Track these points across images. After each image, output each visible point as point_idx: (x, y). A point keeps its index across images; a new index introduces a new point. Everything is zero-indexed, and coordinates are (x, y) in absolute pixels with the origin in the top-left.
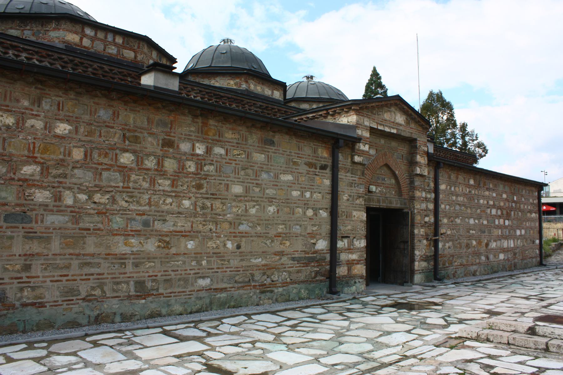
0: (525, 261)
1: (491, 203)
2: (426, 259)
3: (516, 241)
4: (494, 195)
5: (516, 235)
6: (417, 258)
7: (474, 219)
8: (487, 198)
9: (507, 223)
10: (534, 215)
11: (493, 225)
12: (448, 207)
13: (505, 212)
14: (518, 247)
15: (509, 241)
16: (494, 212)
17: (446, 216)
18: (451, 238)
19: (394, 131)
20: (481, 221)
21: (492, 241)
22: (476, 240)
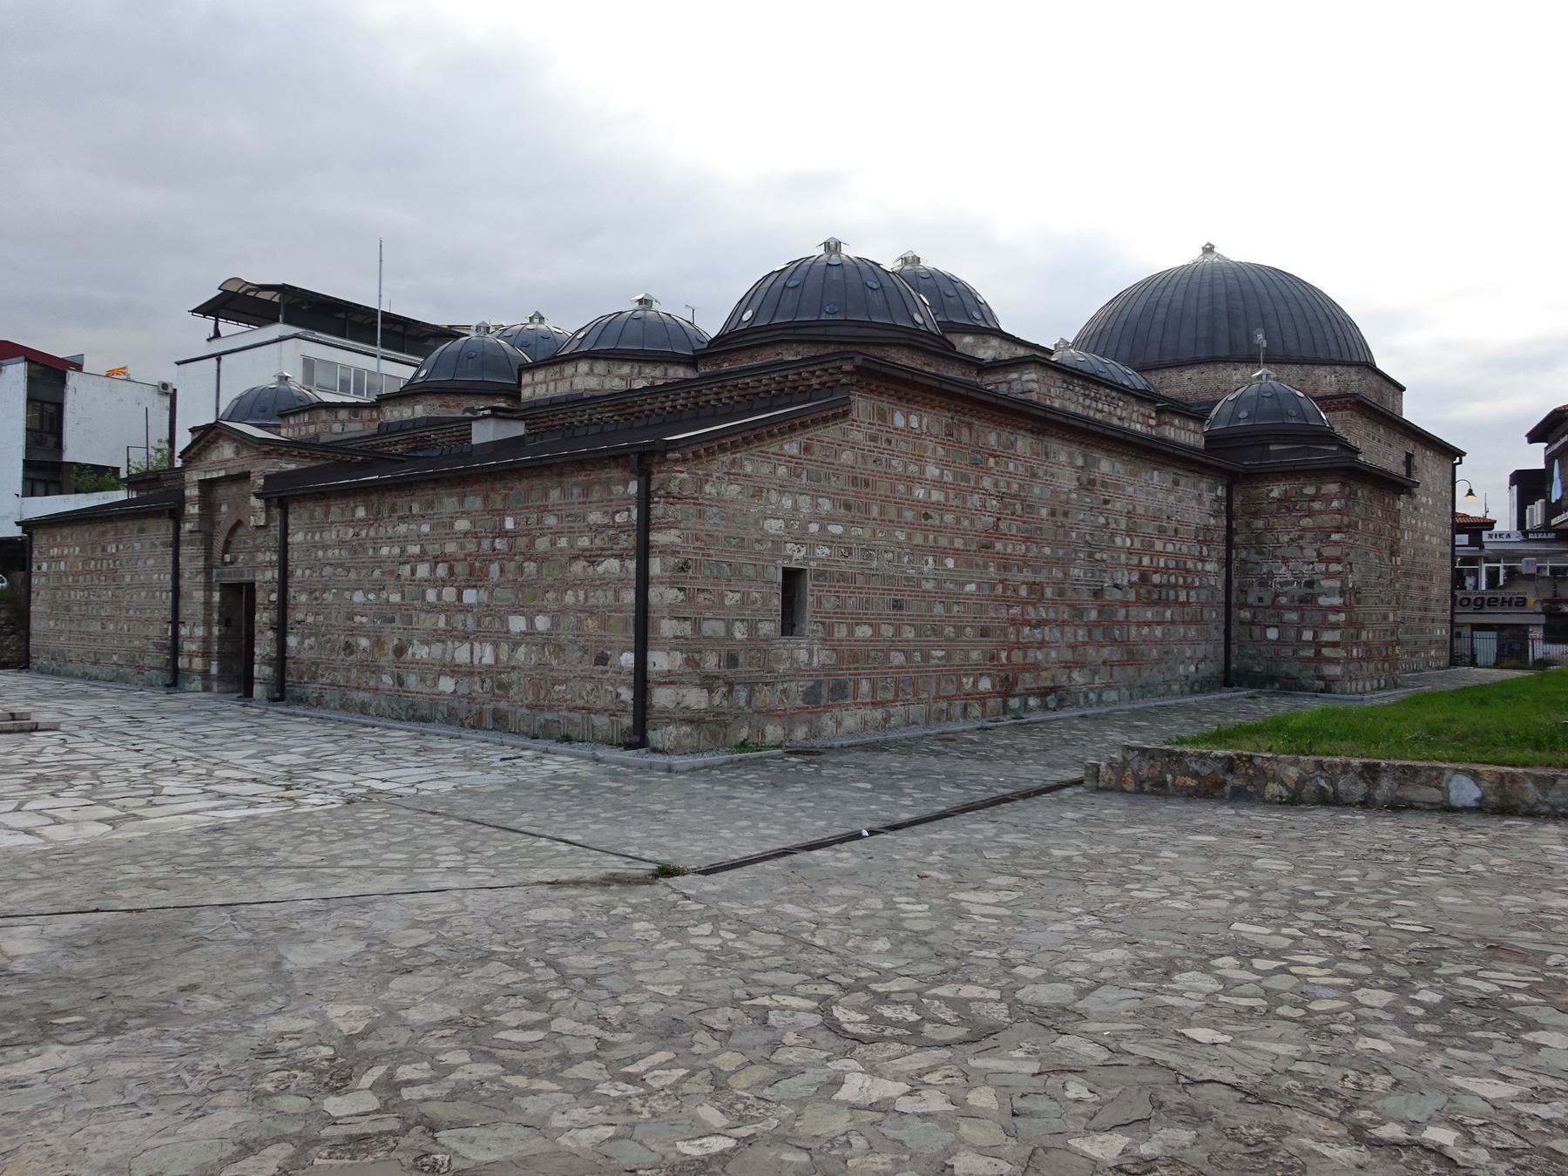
0: (549, 716)
1: (415, 549)
2: (268, 662)
3: (505, 648)
4: (425, 528)
5: (508, 632)
6: (257, 659)
7: (366, 592)
8: (405, 540)
9: (470, 596)
10: (612, 565)
11: (417, 603)
12: (308, 572)
13: (460, 568)
14: (514, 668)
15: (477, 645)
16: (423, 570)
17: (304, 590)
18: (314, 631)
19: (222, 473)
20: (384, 595)
21: (415, 642)
22: (368, 637)
